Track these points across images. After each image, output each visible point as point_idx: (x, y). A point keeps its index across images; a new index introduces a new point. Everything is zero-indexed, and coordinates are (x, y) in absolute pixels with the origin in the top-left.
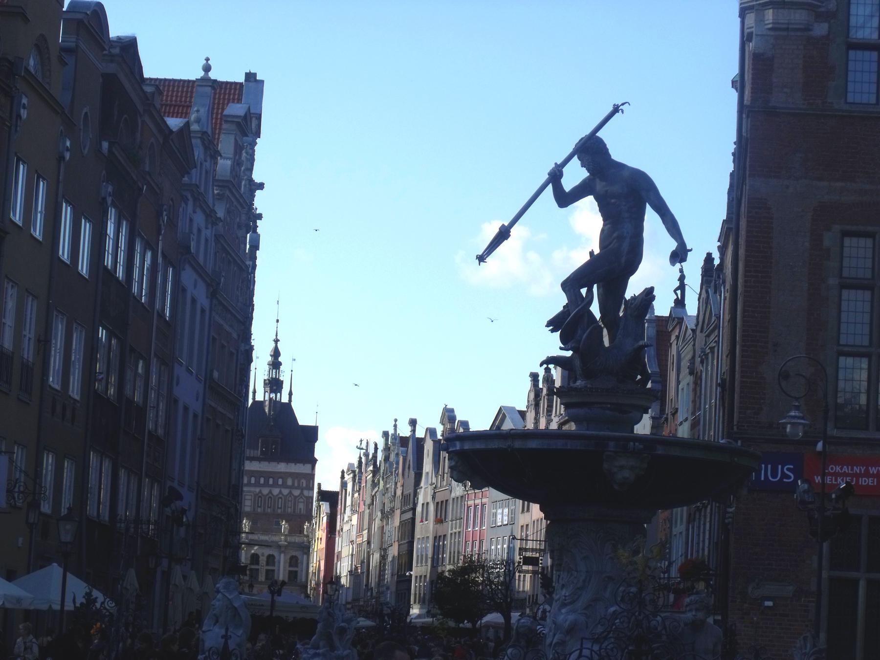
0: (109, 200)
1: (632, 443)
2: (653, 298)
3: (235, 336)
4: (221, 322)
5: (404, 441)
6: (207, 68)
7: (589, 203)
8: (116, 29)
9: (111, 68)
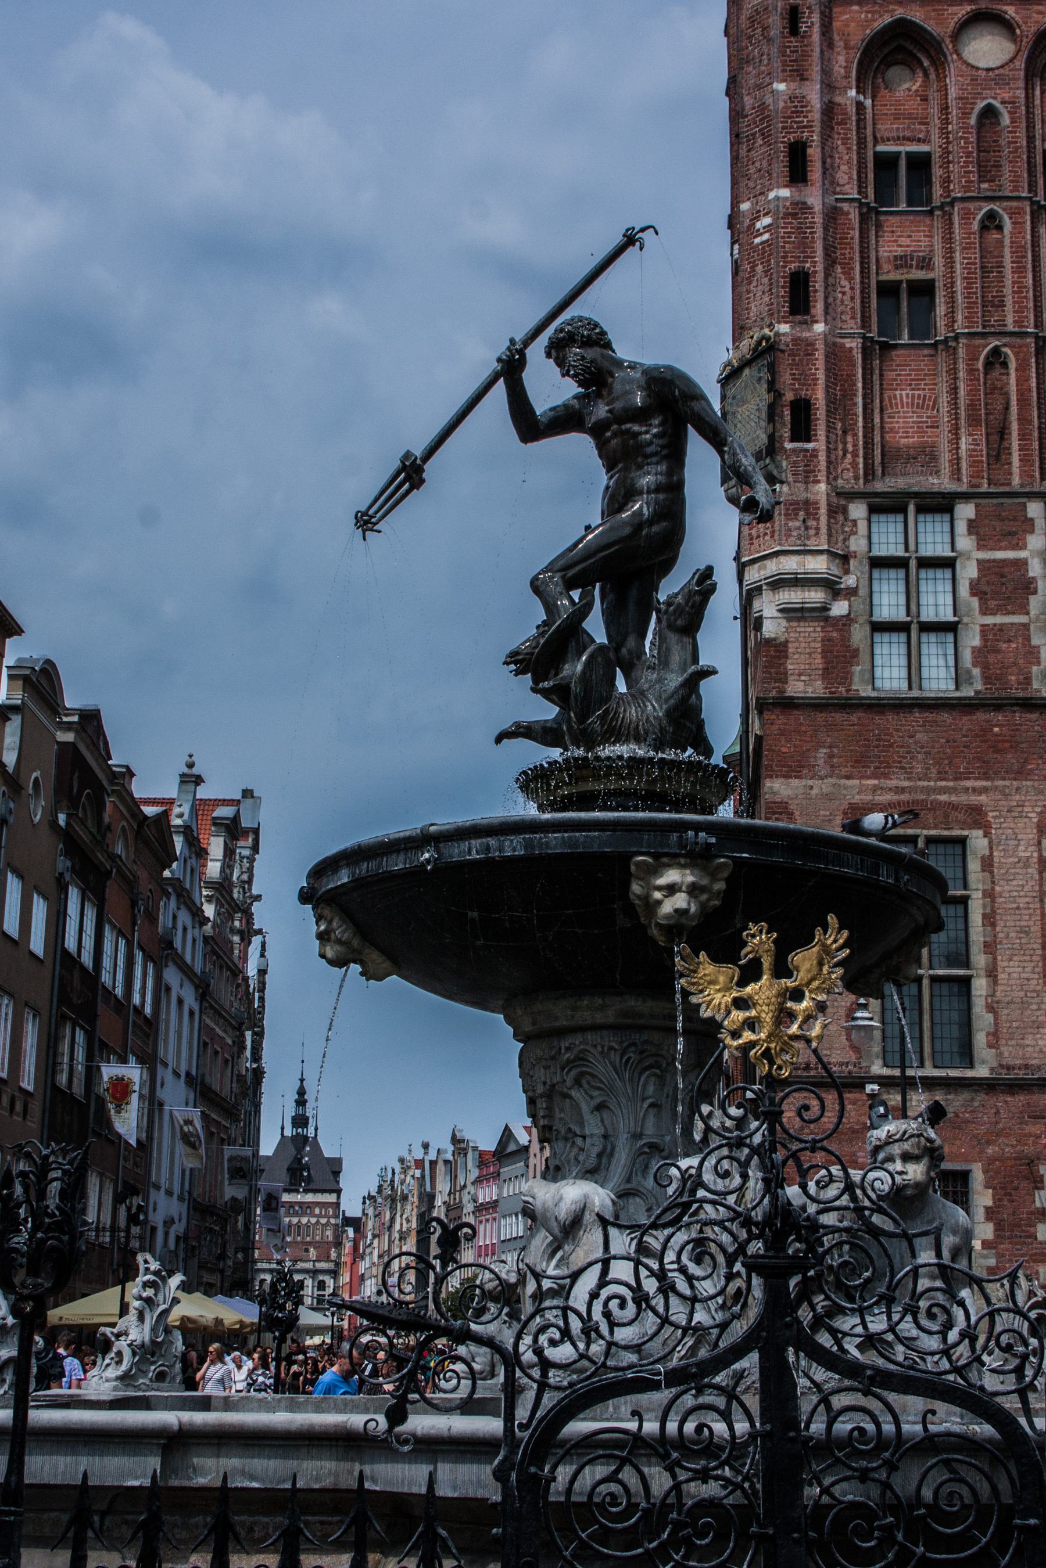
0: (67, 877)
1: (691, 833)
2: (712, 589)
3: (230, 1042)
4: (212, 1025)
5: (420, 1164)
6: (191, 765)
7: (579, 447)
8: (72, 699)
9: (69, 737)
